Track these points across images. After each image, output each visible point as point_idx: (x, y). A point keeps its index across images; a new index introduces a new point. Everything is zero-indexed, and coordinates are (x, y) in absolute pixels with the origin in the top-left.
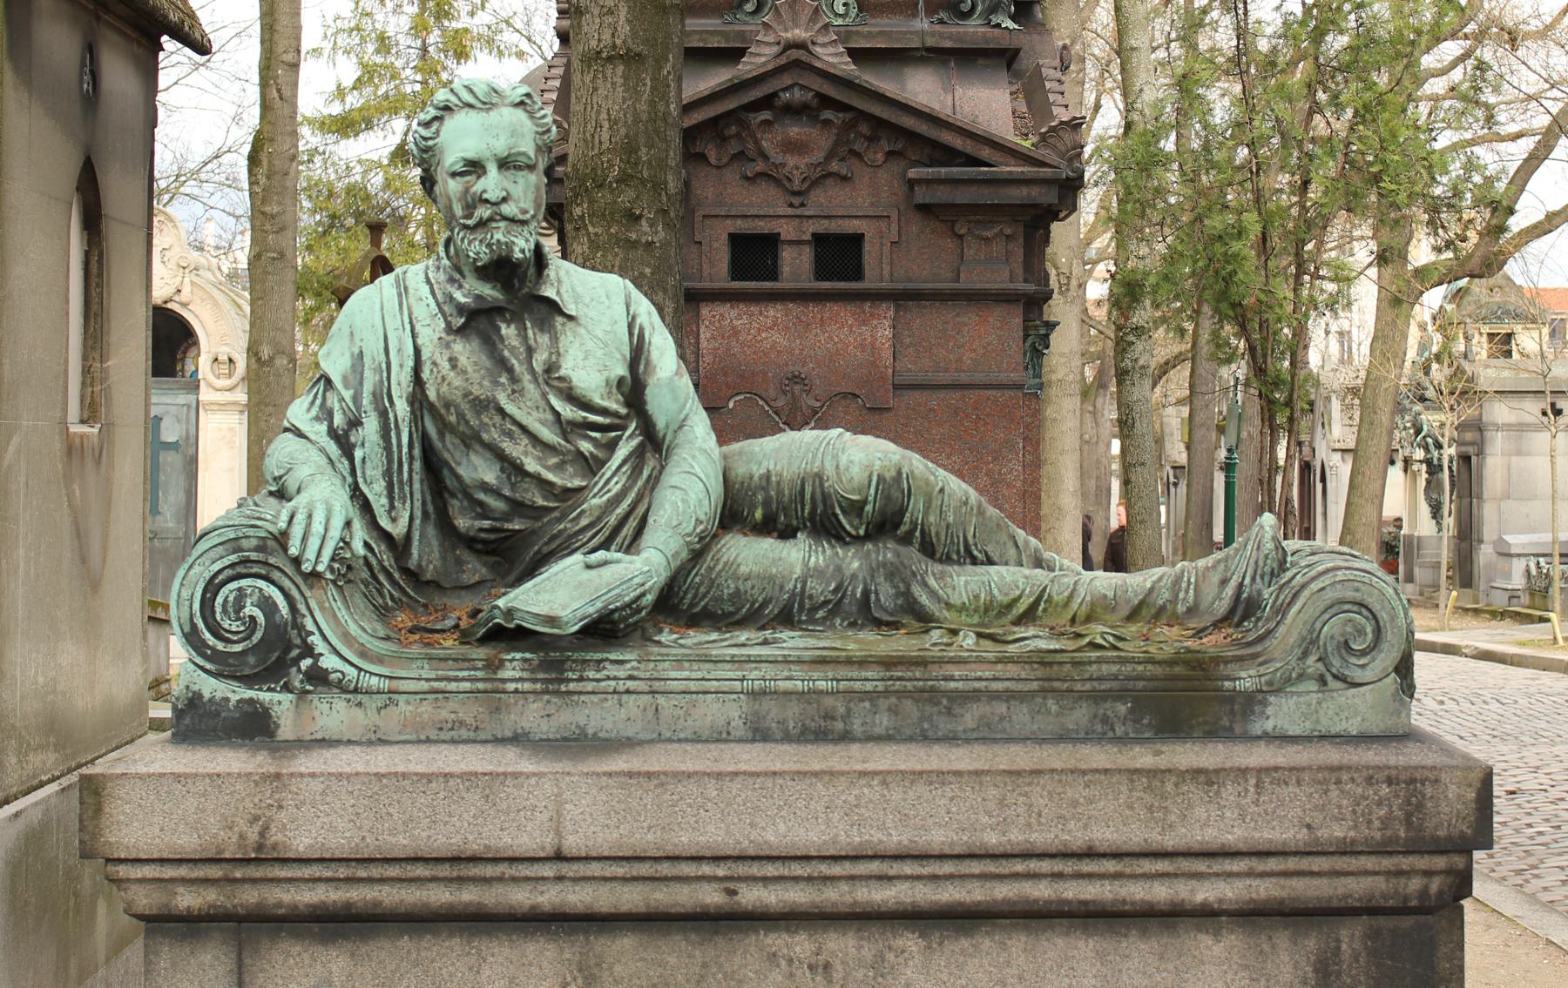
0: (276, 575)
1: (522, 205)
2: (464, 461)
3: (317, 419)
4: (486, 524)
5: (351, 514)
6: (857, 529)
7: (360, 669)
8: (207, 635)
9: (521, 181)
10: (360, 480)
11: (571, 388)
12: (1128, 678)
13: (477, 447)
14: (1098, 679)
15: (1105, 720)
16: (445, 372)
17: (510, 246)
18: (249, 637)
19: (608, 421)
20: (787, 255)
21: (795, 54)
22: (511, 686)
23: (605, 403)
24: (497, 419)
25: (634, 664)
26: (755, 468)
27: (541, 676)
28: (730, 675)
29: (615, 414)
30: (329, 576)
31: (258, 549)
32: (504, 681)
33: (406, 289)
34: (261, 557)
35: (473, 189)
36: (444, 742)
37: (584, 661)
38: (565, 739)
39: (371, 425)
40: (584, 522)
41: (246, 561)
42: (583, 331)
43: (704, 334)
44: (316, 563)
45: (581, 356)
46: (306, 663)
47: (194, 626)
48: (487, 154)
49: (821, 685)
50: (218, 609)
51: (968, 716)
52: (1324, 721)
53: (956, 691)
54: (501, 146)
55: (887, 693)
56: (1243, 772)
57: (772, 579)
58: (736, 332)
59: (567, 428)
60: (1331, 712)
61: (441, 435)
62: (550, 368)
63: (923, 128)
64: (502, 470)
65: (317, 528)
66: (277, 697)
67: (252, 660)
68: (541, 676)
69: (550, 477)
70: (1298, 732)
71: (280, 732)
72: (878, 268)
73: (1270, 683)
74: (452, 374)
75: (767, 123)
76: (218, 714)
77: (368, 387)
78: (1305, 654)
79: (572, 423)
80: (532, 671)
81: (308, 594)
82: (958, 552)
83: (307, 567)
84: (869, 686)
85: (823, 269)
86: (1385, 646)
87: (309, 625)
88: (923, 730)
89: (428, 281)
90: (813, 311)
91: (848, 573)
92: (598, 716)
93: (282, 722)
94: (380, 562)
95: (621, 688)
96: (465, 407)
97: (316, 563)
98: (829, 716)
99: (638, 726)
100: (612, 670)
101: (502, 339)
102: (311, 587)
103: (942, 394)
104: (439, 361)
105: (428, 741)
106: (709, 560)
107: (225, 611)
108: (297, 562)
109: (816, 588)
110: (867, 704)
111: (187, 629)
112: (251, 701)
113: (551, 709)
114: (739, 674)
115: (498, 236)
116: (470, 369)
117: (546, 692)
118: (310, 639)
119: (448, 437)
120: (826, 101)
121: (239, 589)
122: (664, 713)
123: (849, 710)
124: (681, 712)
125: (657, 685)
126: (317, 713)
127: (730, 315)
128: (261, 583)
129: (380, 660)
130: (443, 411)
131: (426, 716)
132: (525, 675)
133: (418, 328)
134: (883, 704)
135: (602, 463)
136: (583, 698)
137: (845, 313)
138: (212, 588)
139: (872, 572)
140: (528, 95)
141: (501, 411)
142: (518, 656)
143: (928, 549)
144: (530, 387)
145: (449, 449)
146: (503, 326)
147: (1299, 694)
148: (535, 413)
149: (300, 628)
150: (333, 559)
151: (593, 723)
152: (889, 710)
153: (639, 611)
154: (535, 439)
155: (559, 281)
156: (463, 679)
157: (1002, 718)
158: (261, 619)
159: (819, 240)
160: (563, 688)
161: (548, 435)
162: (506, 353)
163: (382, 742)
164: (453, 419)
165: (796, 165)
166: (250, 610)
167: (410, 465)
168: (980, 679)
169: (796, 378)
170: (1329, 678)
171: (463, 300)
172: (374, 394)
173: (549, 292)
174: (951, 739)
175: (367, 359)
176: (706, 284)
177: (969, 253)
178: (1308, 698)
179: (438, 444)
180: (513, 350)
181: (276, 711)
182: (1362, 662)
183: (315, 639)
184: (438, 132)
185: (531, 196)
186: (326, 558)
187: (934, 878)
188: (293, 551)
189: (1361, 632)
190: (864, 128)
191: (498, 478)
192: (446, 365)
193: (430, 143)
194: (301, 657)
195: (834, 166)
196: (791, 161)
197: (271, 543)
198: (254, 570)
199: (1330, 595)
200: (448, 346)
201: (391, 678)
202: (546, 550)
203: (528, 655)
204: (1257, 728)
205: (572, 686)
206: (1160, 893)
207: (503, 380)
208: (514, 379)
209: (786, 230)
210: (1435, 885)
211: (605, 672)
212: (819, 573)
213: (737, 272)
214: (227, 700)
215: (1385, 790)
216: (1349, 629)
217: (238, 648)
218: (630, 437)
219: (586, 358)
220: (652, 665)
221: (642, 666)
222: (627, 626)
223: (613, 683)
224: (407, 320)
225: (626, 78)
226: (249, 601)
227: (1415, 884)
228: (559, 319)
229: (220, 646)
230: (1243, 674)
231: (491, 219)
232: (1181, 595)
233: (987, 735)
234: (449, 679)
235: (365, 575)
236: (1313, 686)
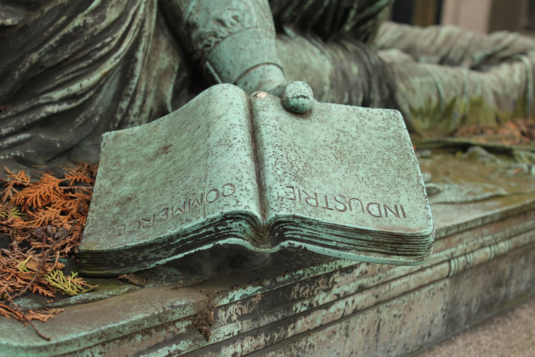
27: (265, 321)
68: (265, 321)
80: (254, 316)
132: (246, 326)
136: (311, 340)
202: (49, 61)
203: (250, 290)
205: (301, 325)
211: (336, 290)
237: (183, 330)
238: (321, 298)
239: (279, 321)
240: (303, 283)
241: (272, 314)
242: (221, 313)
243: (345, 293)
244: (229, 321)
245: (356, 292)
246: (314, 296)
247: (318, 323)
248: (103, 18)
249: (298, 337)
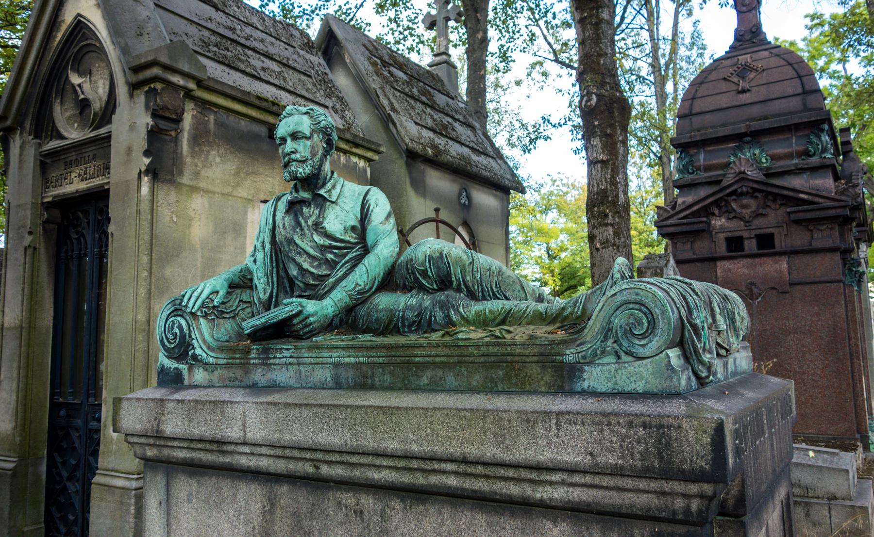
1: (303, 154)
6: (432, 285)
8: (165, 341)
9: (302, 144)
12: (503, 355)
14: (487, 356)
15: (492, 380)
17: (296, 172)
20: (746, 243)
21: (742, 175)
22: (252, 361)
28: (326, 355)
29: (349, 242)
36: (231, 387)
38: (269, 387)
40: (326, 289)
42: (338, 208)
43: (719, 271)
49: (361, 359)
51: (425, 378)
52: (620, 383)
53: (418, 362)
54: (291, 129)
55: (389, 364)
56: (548, 413)
57: (391, 310)
58: (730, 270)
59: (323, 249)
60: (624, 377)
63: (790, 194)
65: (196, 294)
67: (177, 351)
69: (313, 270)
70: (604, 390)
72: (780, 243)
73: (584, 357)
75: (734, 200)
78: (606, 338)
79: (322, 246)
80: (259, 354)
82: (490, 296)
84: (381, 360)
85: (760, 246)
86: (658, 331)
87: (193, 336)
88: (405, 385)
90: (757, 260)
91: (424, 306)
92: (281, 376)
98: (365, 377)
101: (302, 214)
103: (809, 286)
105: (227, 386)
106: (368, 305)
109: (409, 314)
110: (380, 370)
115: (293, 168)
117: (263, 364)
120: (755, 190)
122: (303, 374)
123: (373, 373)
127: (727, 264)
128: (179, 318)
134: (387, 370)
135: (337, 263)
137: (769, 261)
139: (434, 305)
141: (295, 243)
143: (472, 295)
144: (307, 232)
147: (603, 365)
148: (309, 244)
149: (190, 336)
152: (390, 373)
154: (309, 255)
157: (441, 379)
158: (178, 334)
159: (759, 237)
161: (312, 252)
162: (301, 218)
163: (213, 386)
165: (746, 212)
168: (429, 356)
169: (752, 284)
170: (623, 355)
174: (417, 390)
176: (718, 255)
177: (815, 236)
178: (609, 367)
182: (642, 342)
183: (195, 342)
186: (196, 307)
187: (410, 470)
189: (639, 322)
190: (770, 197)
192: (281, 227)
195: (760, 211)
196: (744, 211)
199: (619, 298)
204: (578, 387)
205: (272, 361)
206: (515, 490)
208: (302, 230)
209: (745, 234)
210: (695, 505)
212: (411, 308)
213: (729, 249)
215: (642, 432)
216: (631, 321)
217: (172, 346)
225: (602, 168)
227: (679, 503)
228: (328, 203)
230: (568, 352)
231: (289, 162)
232: (576, 310)
233: (434, 388)
236: (612, 359)
238: (278, 355)
249: (271, 364)
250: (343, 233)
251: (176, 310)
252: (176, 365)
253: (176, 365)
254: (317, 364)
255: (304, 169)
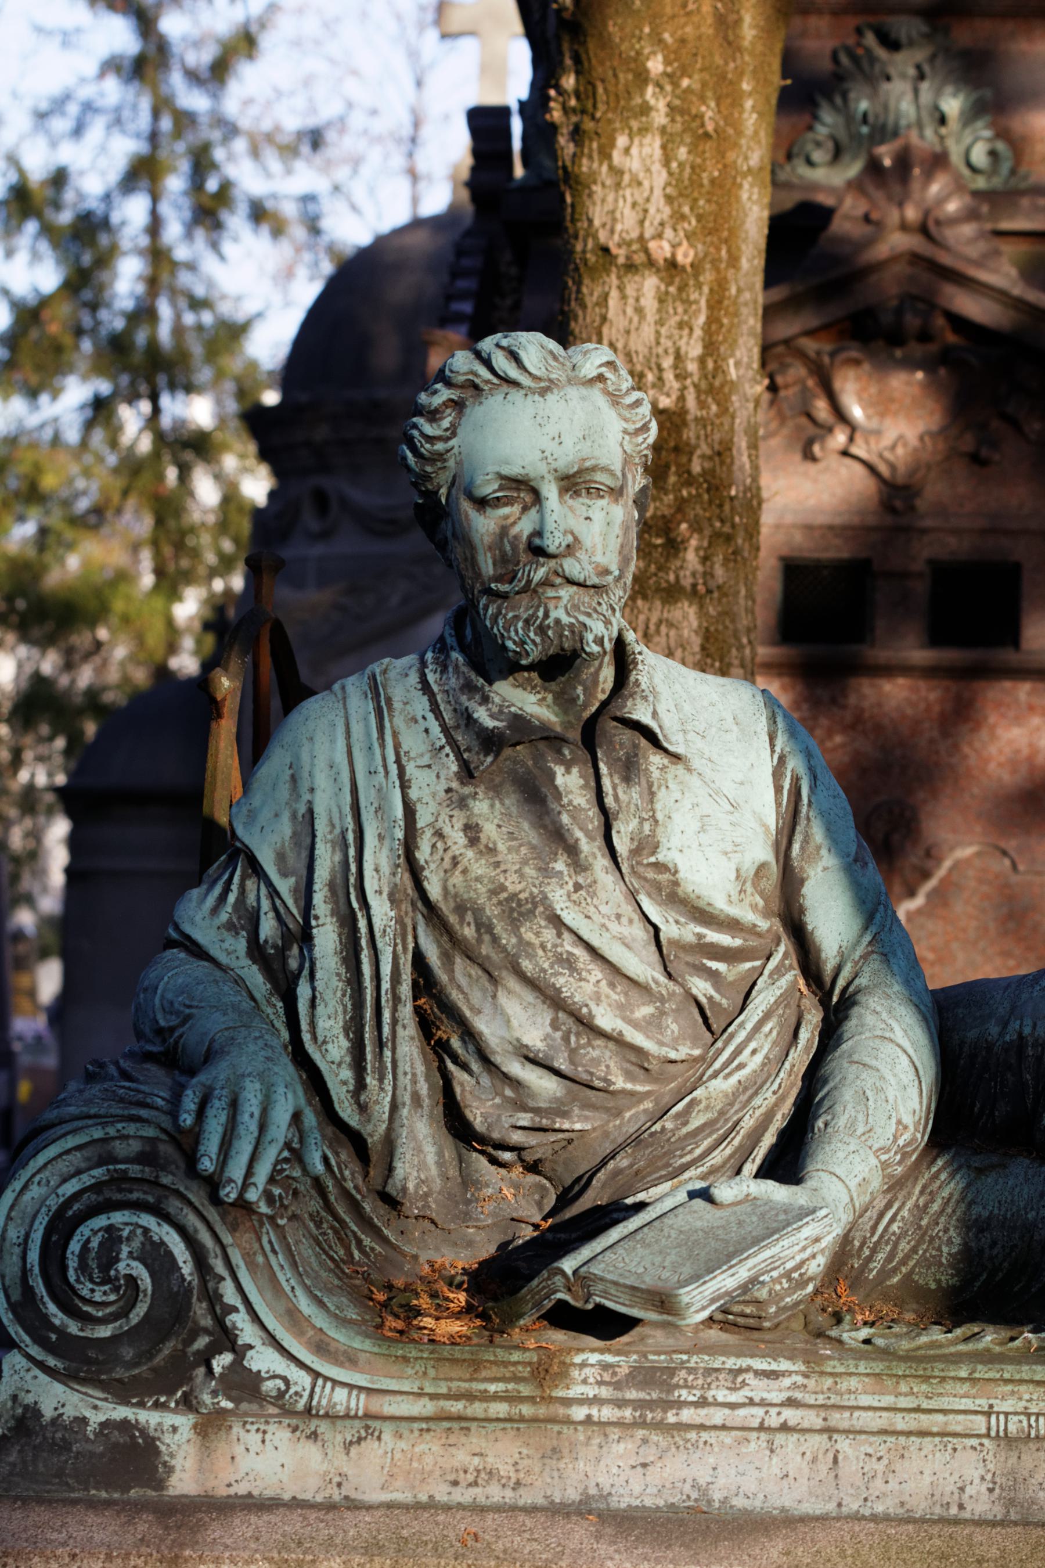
0: (173, 1205)
1: (599, 558)
2: (487, 1009)
3: (230, 927)
4: (525, 1119)
5: (302, 1101)
7: (316, 1375)
8: (52, 1308)
9: (597, 515)
10: (306, 1037)
11: (676, 883)
13: (512, 982)
16: (456, 850)
18: (124, 1313)
19: (737, 942)
22: (579, 1413)
23: (735, 911)
24: (549, 934)
25: (799, 1379)
26: (994, 1030)
27: (632, 1394)
28: (966, 1404)
30: (264, 1208)
31: (141, 1159)
32: (568, 1402)
33: (389, 701)
34: (148, 1172)
35: (515, 530)
37: (709, 1371)
39: (327, 938)
40: (697, 1121)
41: (120, 1180)
42: (694, 781)
44: (246, 1185)
45: (695, 825)
46: (221, 1362)
47: (28, 1291)
48: (542, 469)
50: (72, 1263)
54: (567, 456)
61: (447, 958)
62: (646, 845)
64: (555, 1025)
66: (170, 1419)
68: (632, 1394)
69: (638, 1038)
71: (174, 1480)
74: (470, 854)
76: (65, 1446)
77: (323, 873)
80: (617, 1386)
81: (227, 1239)
83: (229, 1193)
89: (425, 687)
93: (177, 1463)
94: (339, 1183)
95: (774, 1421)
96: (492, 911)
97: (246, 1185)
99: (802, 1488)
100: (758, 1388)
101: (558, 795)
102: (233, 1228)
104: (447, 830)
107: (83, 1266)
108: (213, 1184)
111: (16, 1295)
112: (125, 1425)
113: (650, 1454)
114: (983, 1403)
116: (501, 847)
117: (643, 1424)
118: (234, 1317)
119: (459, 962)
121: (110, 1229)
122: (849, 1468)
124: (880, 1467)
125: (838, 1419)
126: (239, 1450)
128: (148, 1220)
129: (349, 1360)
130: (453, 919)
131: (429, 1460)
132: (605, 1392)
133: (410, 769)
136: (705, 1435)
138: (62, 1225)
140: (610, 364)
141: (557, 922)
142: (594, 1358)
145: (462, 984)
146: (559, 770)
148: (614, 926)
149: (213, 1299)
150: (271, 1180)
151: (721, 1481)
153: (802, 1283)
155: (654, 692)
156: (496, 1397)
158: (146, 1281)
160: (671, 1418)
162: (565, 819)
164: (469, 932)
166: (129, 1266)
167: (395, 1010)
171: (490, 723)
172: (331, 885)
173: (642, 714)
175: (321, 827)
179: (443, 977)
180: (575, 812)
181: (168, 1443)
183: (240, 1320)
184: (453, 431)
185: (614, 544)
186: (261, 1176)
188: (207, 1165)
191: (546, 1038)
192: (457, 838)
193: (440, 446)
194: (214, 1349)
197: (166, 1149)
198: (135, 1196)
200: (462, 803)
201: (369, 1391)
205: (687, 1415)
207: (560, 866)
208: (578, 864)
211: (746, 1392)
214: (84, 1421)
217: (104, 1332)
218: (779, 972)
219: (703, 829)
220: (829, 1382)
221: (811, 1383)
222: (781, 1310)
223: (759, 1412)
224: (391, 757)
226: (125, 1250)
228: (656, 760)
229: (74, 1328)
234: (470, 1397)
235: (315, 1204)
237: (526, 1374)
239: (652, 1401)
240: (691, 1371)
241: (642, 1390)
242: (575, 1373)
243: (762, 1400)
244: (585, 1381)
245: (782, 1405)
246: (709, 1388)
247: (718, 1420)
248: (685, 1123)
250: (735, 897)
251: (120, 1180)
252: (121, 1412)
253: (121, 1412)
254: (923, 1434)
255: (607, 623)
